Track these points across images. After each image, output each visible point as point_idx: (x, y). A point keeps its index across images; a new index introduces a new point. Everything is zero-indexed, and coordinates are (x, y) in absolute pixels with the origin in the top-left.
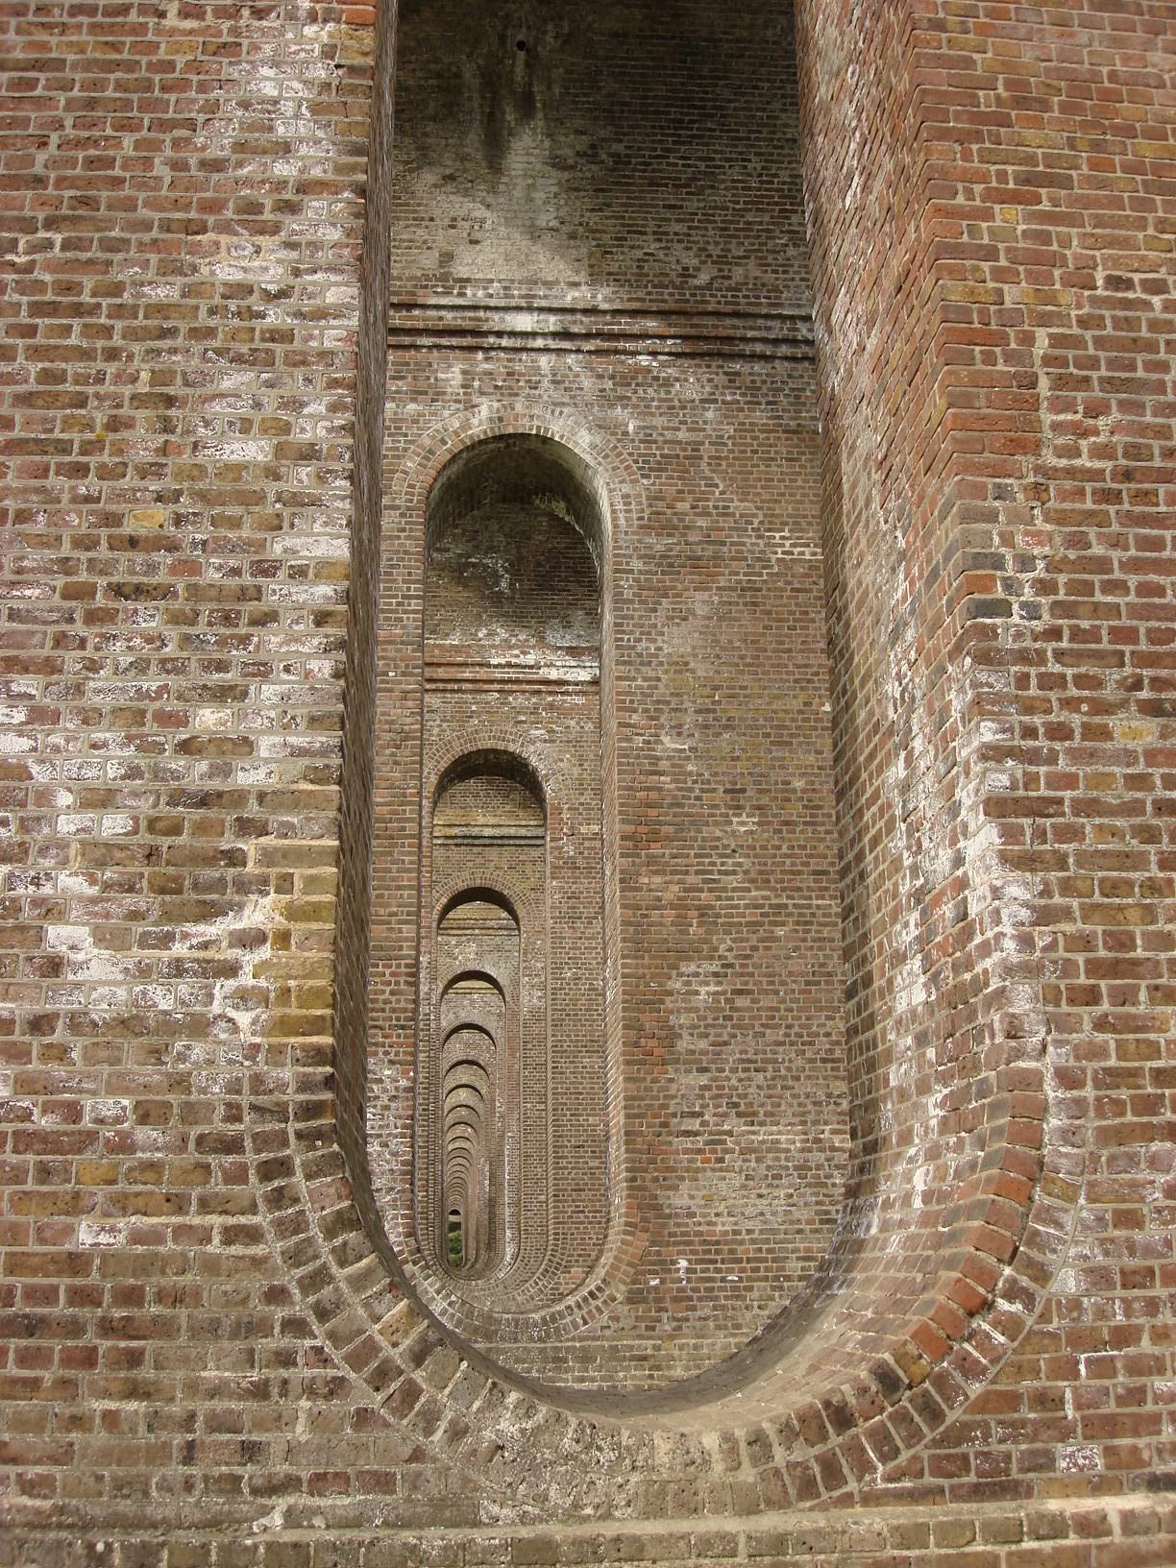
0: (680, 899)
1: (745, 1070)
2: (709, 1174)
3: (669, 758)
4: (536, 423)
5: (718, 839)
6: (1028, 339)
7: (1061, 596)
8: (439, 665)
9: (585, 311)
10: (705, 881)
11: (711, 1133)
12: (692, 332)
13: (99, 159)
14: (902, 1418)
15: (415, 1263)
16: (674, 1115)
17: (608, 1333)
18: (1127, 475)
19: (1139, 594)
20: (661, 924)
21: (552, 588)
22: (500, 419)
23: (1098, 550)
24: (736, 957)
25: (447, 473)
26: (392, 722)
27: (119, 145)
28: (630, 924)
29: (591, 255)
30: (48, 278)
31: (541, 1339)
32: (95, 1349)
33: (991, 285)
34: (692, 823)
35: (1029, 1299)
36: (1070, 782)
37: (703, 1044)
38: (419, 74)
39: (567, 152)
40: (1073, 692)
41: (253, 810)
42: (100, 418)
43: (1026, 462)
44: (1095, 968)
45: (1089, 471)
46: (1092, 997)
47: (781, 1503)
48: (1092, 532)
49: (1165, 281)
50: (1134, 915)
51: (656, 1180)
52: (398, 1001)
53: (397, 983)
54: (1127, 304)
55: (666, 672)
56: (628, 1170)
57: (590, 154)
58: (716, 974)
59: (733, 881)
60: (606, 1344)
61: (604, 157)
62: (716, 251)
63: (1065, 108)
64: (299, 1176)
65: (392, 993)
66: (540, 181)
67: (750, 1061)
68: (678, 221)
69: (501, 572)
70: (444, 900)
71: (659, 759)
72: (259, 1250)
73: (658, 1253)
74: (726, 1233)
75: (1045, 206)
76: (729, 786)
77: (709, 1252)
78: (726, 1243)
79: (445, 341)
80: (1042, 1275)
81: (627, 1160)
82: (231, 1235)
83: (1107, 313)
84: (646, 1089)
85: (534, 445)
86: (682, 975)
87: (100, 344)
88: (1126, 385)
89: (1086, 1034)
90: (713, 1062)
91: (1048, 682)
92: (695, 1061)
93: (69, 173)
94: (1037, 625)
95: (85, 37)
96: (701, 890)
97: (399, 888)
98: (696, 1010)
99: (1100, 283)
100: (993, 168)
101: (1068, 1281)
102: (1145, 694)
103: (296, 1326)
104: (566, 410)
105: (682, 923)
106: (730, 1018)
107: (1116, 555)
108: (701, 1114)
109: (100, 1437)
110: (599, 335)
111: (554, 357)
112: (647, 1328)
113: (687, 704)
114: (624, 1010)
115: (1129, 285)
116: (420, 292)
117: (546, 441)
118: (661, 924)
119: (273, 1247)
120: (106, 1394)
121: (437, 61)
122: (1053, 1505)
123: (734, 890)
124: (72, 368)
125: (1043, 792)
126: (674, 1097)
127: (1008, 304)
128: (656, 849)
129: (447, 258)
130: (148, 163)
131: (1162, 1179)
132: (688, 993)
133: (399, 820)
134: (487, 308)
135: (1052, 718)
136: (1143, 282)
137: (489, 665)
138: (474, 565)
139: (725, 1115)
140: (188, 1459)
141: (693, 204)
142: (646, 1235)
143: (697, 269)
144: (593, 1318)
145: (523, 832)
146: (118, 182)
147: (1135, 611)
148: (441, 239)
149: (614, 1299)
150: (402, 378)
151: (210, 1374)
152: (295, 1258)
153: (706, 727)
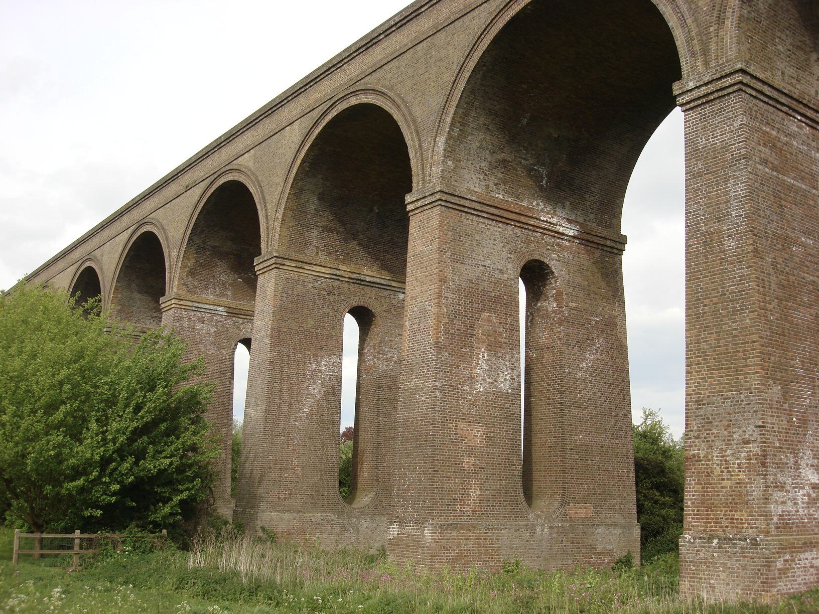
8: (522, 215)
137: (539, 220)
138: (536, 170)
145: (382, 282)
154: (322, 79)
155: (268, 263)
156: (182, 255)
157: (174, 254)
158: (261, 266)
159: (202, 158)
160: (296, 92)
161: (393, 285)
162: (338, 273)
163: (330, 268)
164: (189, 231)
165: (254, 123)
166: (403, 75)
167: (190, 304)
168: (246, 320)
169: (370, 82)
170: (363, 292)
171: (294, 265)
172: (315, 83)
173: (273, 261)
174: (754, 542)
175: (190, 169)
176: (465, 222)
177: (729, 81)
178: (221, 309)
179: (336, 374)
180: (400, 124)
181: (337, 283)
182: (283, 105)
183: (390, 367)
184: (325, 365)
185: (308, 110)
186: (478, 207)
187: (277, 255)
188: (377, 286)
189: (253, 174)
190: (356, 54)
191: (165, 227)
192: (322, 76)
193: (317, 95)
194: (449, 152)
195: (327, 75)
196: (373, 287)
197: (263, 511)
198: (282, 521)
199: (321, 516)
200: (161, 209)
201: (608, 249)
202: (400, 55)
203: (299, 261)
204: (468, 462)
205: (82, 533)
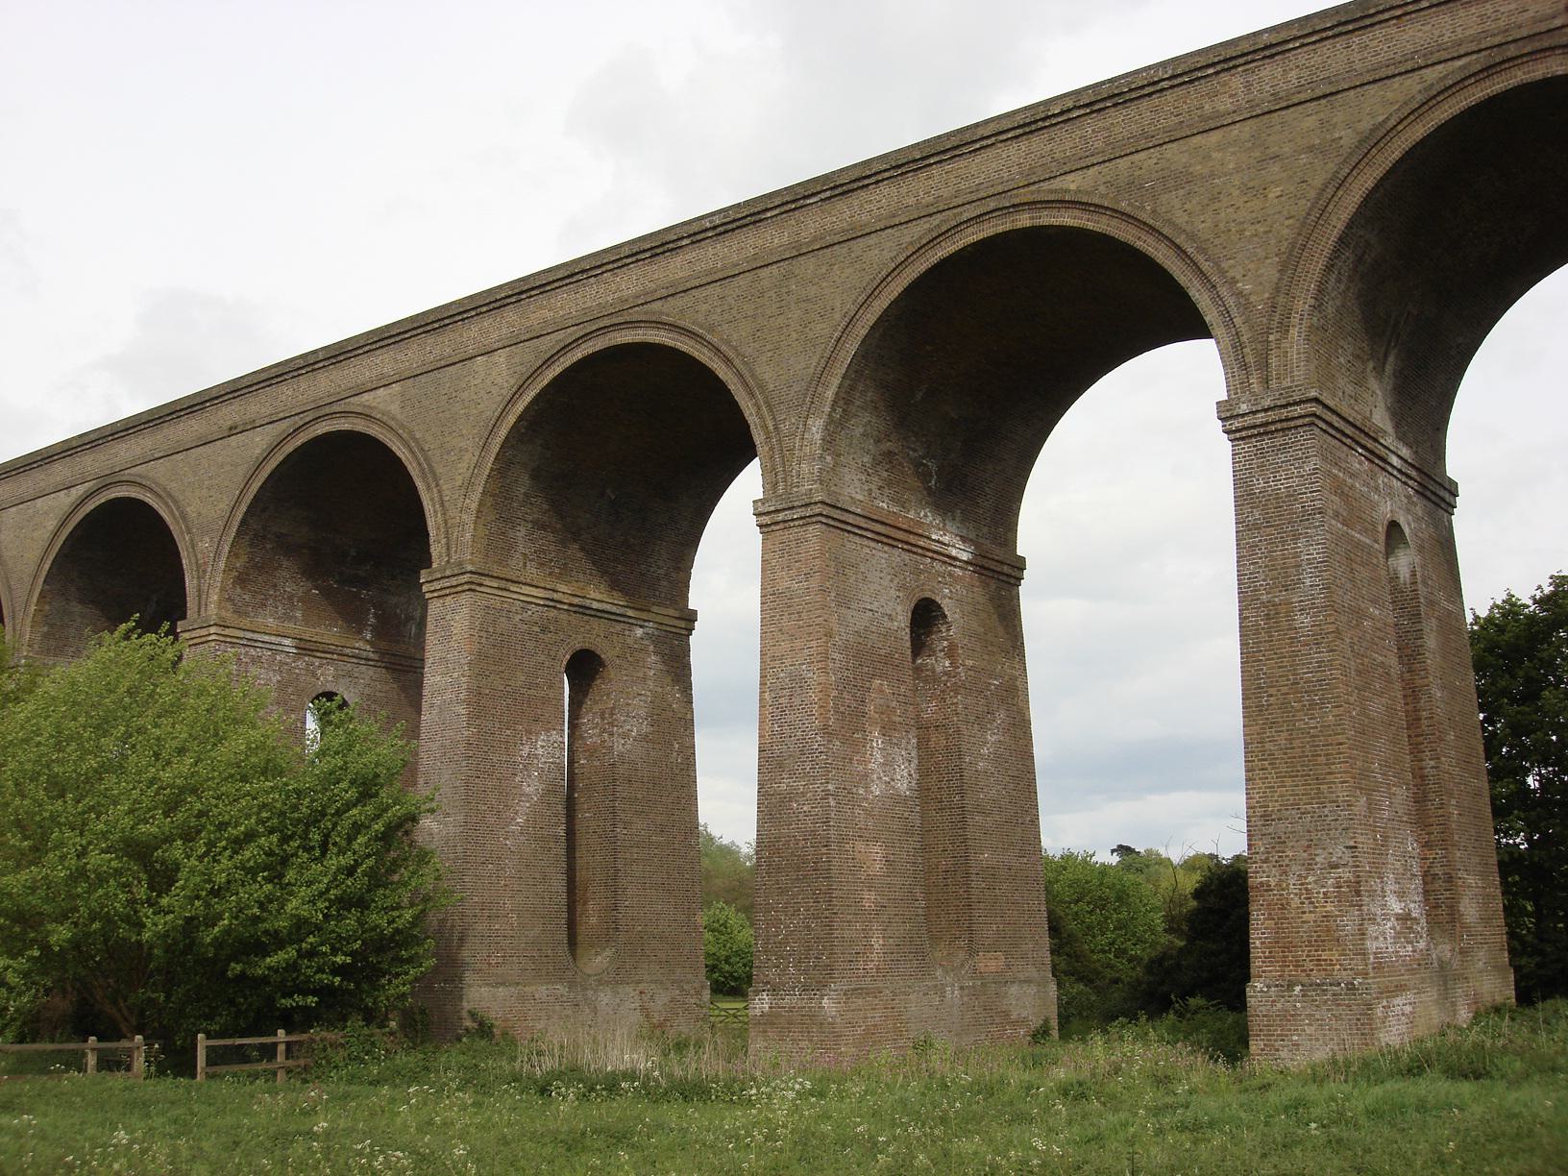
21: (950, 491)
137: (929, 538)
145: (614, 609)
154: (557, 288)
155: (454, 581)
156: (227, 549)
157: (205, 544)
158: (437, 585)
159: (268, 383)
160: (496, 301)
161: (628, 614)
162: (555, 596)
163: (545, 588)
164: (243, 508)
165: (397, 339)
166: (733, 312)
167: (241, 634)
168: (325, 661)
169: (669, 310)
171: (496, 585)
172: (541, 293)
173: (466, 578)
174: (1351, 987)
175: (234, 398)
176: (848, 545)
177: (1299, 410)
178: (287, 642)
179: (558, 761)
180: (732, 387)
181: (553, 613)
182: (467, 318)
183: (628, 747)
184: (542, 747)
185: (528, 336)
186: (863, 523)
187: (473, 569)
188: (606, 616)
189: (403, 426)
190: (630, 260)
191: (175, 494)
192: (556, 285)
193: (549, 315)
194: (829, 442)
195: (567, 285)
196: (601, 617)
197: (470, 986)
198: (495, 1001)
199: (547, 989)
200: (161, 461)
201: (1005, 578)
202: (724, 279)
203: (502, 579)
204: (869, 899)
205: (288, 1033)
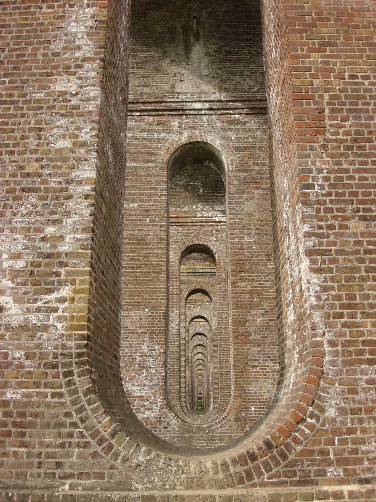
0: (251, 290)
1: (273, 345)
2: (261, 379)
3: (247, 244)
4: (202, 138)
5: (263, 270)
6: (322, 97)
7: (332, 182)
8: (181, 217)
9: (217, 101)
10: (259, 284)
11: (262, 366)
12: (252, 106)
13: (21, 54)
14: (273, 458)
15: (166, 408)
16: (250, 360)
17: (228, 431)
18: (355, 141)
19: (359, 180)
20: (245, 298)
21: (216, 192)
22: (191, 137)
23: (345, 166)
24: (270, 309)
25: (174, 155)
26: (157, 235)
27: (27, 50)
28: (235, 298)
29: (219, 83)
30: (4, 93)
31: (207, 433)
32: (11, 431)
33: (309, 79)
34: (254, 265)
35: (318, 418)
36: (334, 244)
37: (259, 337)
38: (163, 28)
39: (211, 50)
40: (336, 214)
41: (64, 259)
42: (19, 136)
43: (320, 137)
44: (342, 306)
45: (342, 139)
46: (341, 316)
47: (232, 486)
48: (343, 160)
49: (369, 76)
50: (356, 288)
51: (244, 381)
52: (160, 324)
53: (160, 318)
54: (356, 84)
55: (246, 216)
56: (235, 378)
57: (218, 51)
58: (263, 314)
59: (268, 284)
60: (228, 435)
61: (223, 51)
62: (260, 80)
63: (335, 20)
64: (76, 377)
65: (158, 322)
66: (202, 60)
67: (274, 343)
68: (247, 71)
69: (200, 187)
70: (187, 293)
71: (243, 245)
72: (63, 400)
73: (245, 405)
74: (267, 399)
75: (328, 53)
76: (266, 253)
77: (261, 405)
78: (267, 402)
79: (173, 113)
80: (322, 410)
81: (234, 375)
82: (54, 395)
83: (349, 87)
84: (240, 352)
85: (202, 145)
86: (252, 315)
87: (19, 113)
88: (355, 111)
89: (339, 328)
90: (262, 343)
91: (327, 210)
92: (256, 343)
93: (11, 59)
94: (324, 192)
95: (17, 17)
96: (258, 287)
97: (160, 288)
98: (257, 326)
99: (347, 77)
100: (311, 41)
101: (331, 412)
102: (361, 214)
103: (74, 425)
104: (212, 133)
105: (251, 298)
106: (268, 329)
107: (351, 167)
108: (258, 360)
109: (12, 459)
110: (222, 109)
111: (208, 116)
112: (241, 430)
113: (252, 227)
114: (233, 326)
115: (357, 77)
116: (165, 97)
117: (206, 143)
118: (245, 298)
119: (67, 399)
120: (14, 446)
121: (168, 24)
122: (325, 488)
123: (268, 287)
124: (10, 120)
125: (325, 247)
126: (249, 354)
127: (315, 86)
128: (243, 274)
129: (173, 86)
130: (36, 55)
131: (365, 378)
132: (254, 320)
133: (160, 266)
134: (186, 102)
135: (328, 222)
136: (362, 76)
137: (197, 217)
138: (191, 185)
139: (266, 360)
140: (39, 467)
141: (252, 65)
142: (241, 399)
143: (254, 86)
144: (224, 426)
146: (26, 61)
147: (357, 186)
148: (171, 80)
149: (230, 420)
150: (159, 125)
151: (47, 440)
152: (74, 402)
153: (259, 234)
170: (198, 280)
